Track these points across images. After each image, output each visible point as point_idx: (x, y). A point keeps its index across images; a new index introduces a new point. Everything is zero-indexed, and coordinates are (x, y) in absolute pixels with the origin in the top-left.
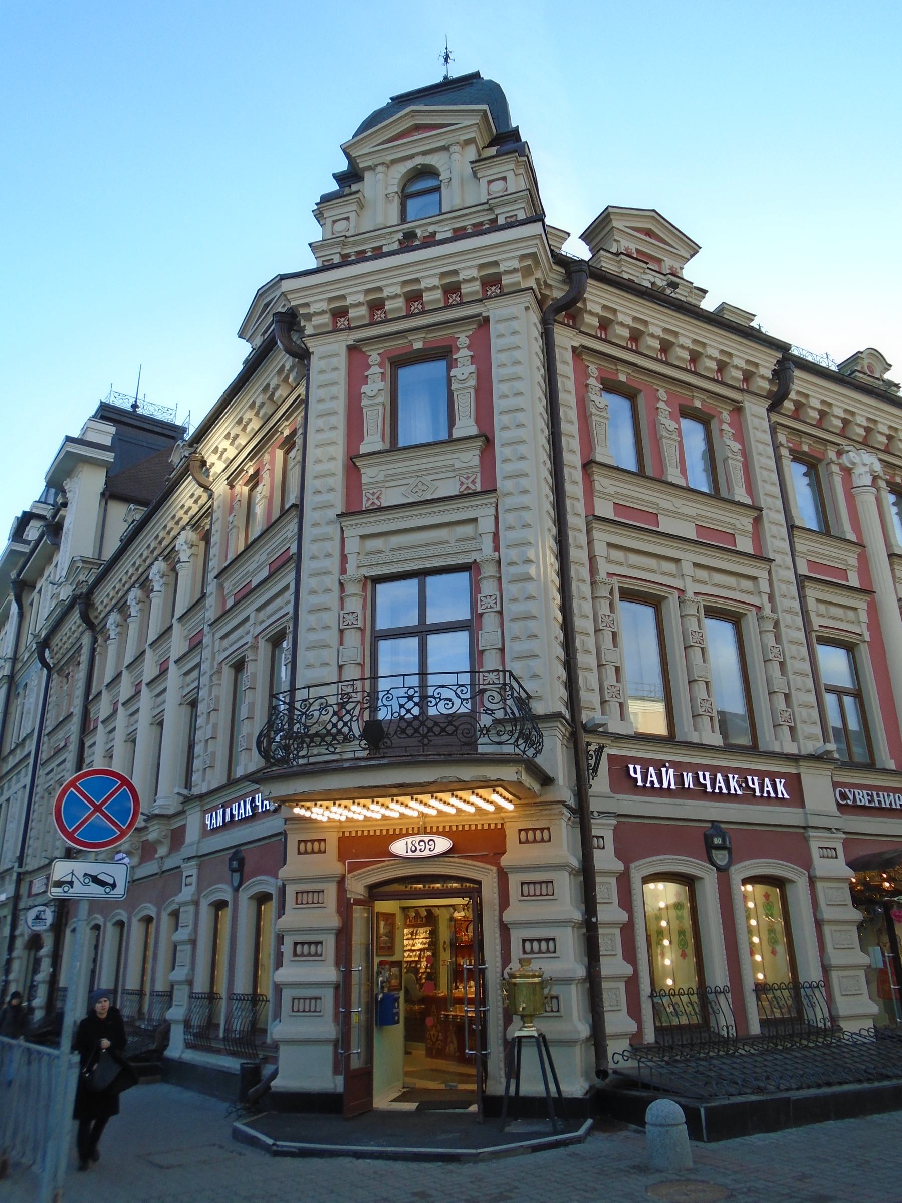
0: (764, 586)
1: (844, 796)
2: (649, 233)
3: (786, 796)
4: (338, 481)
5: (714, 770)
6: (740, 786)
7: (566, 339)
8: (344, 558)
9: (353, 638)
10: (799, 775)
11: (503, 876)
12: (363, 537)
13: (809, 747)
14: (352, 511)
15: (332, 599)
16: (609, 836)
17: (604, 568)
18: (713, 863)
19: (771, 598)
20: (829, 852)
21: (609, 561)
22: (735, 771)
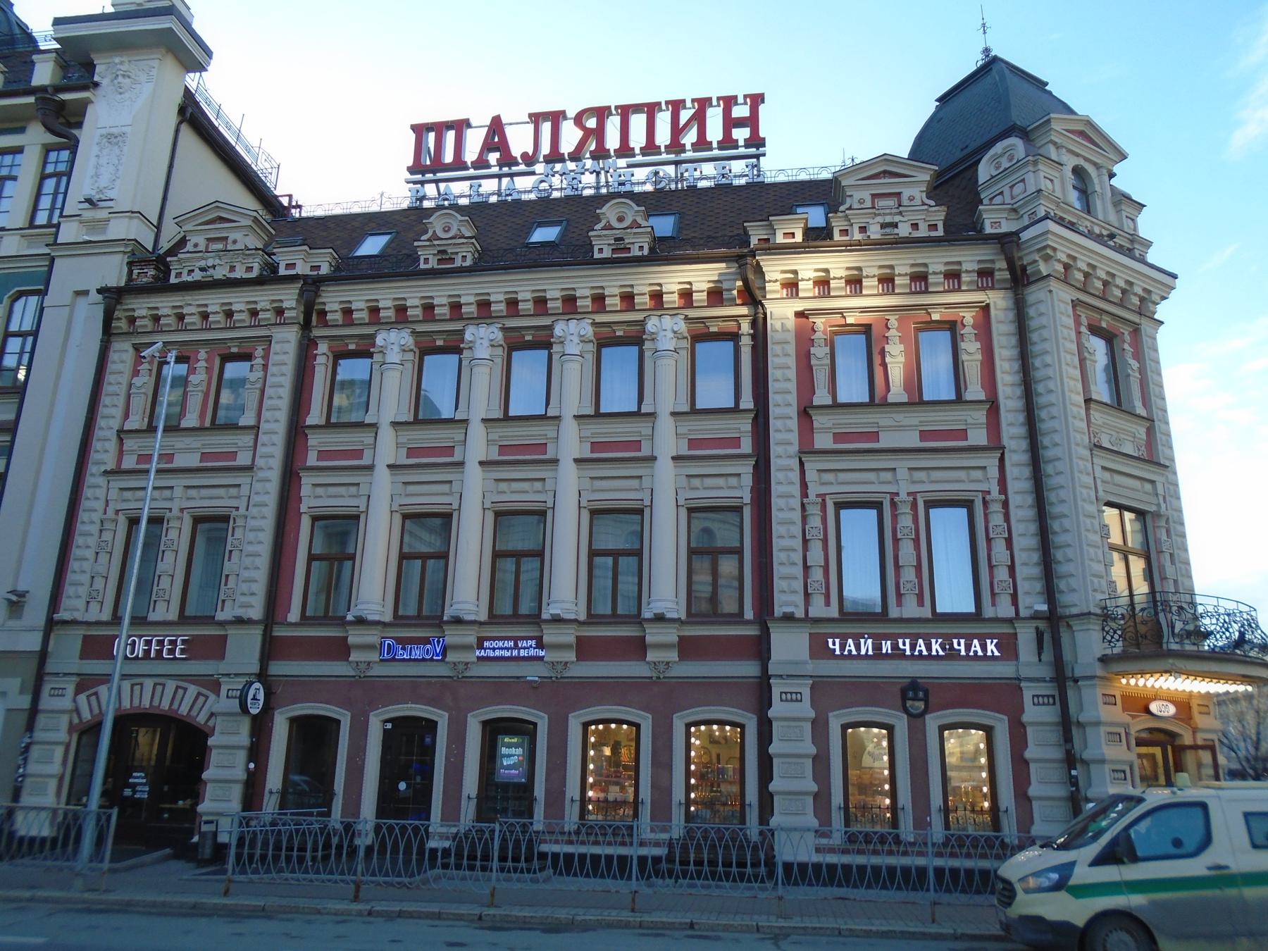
0: (994, 472)
3: (997, 653)
5: (914, 638)
6: (944, 649)
16: (806, 693)
17: (812, 491)
18: (906, 710)
22: (937, 636)
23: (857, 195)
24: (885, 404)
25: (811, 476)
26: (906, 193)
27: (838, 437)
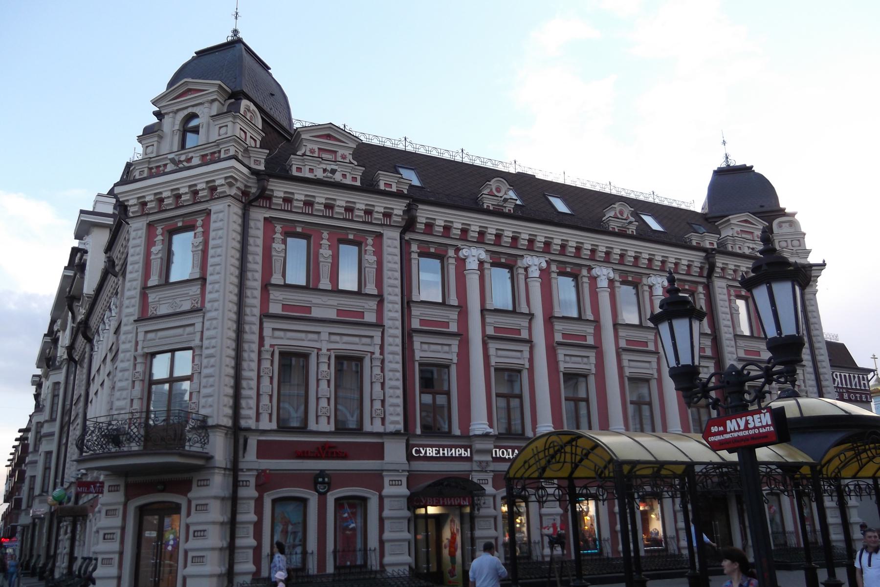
0: (378, 340)
1: (418, 452)
2: (329, 136)
4: (136, 301)
7: (258, 215)
8: (137, 343)
9: (138, 386)
10: (383, 443)
11: (189, 502)
12: (146, 332)
13: (391, 428)
14: (143, 318)
15: (128, 365)
16: (253, 481)
17: (268, 342)
18: (317, 491)
19: (382, 347)
20: (395, 483)
21: (273, 337)
23: (310, 146)
24: (316, 289)
25: (267, 332)
26: (341, 152)
27: (285, 307)
